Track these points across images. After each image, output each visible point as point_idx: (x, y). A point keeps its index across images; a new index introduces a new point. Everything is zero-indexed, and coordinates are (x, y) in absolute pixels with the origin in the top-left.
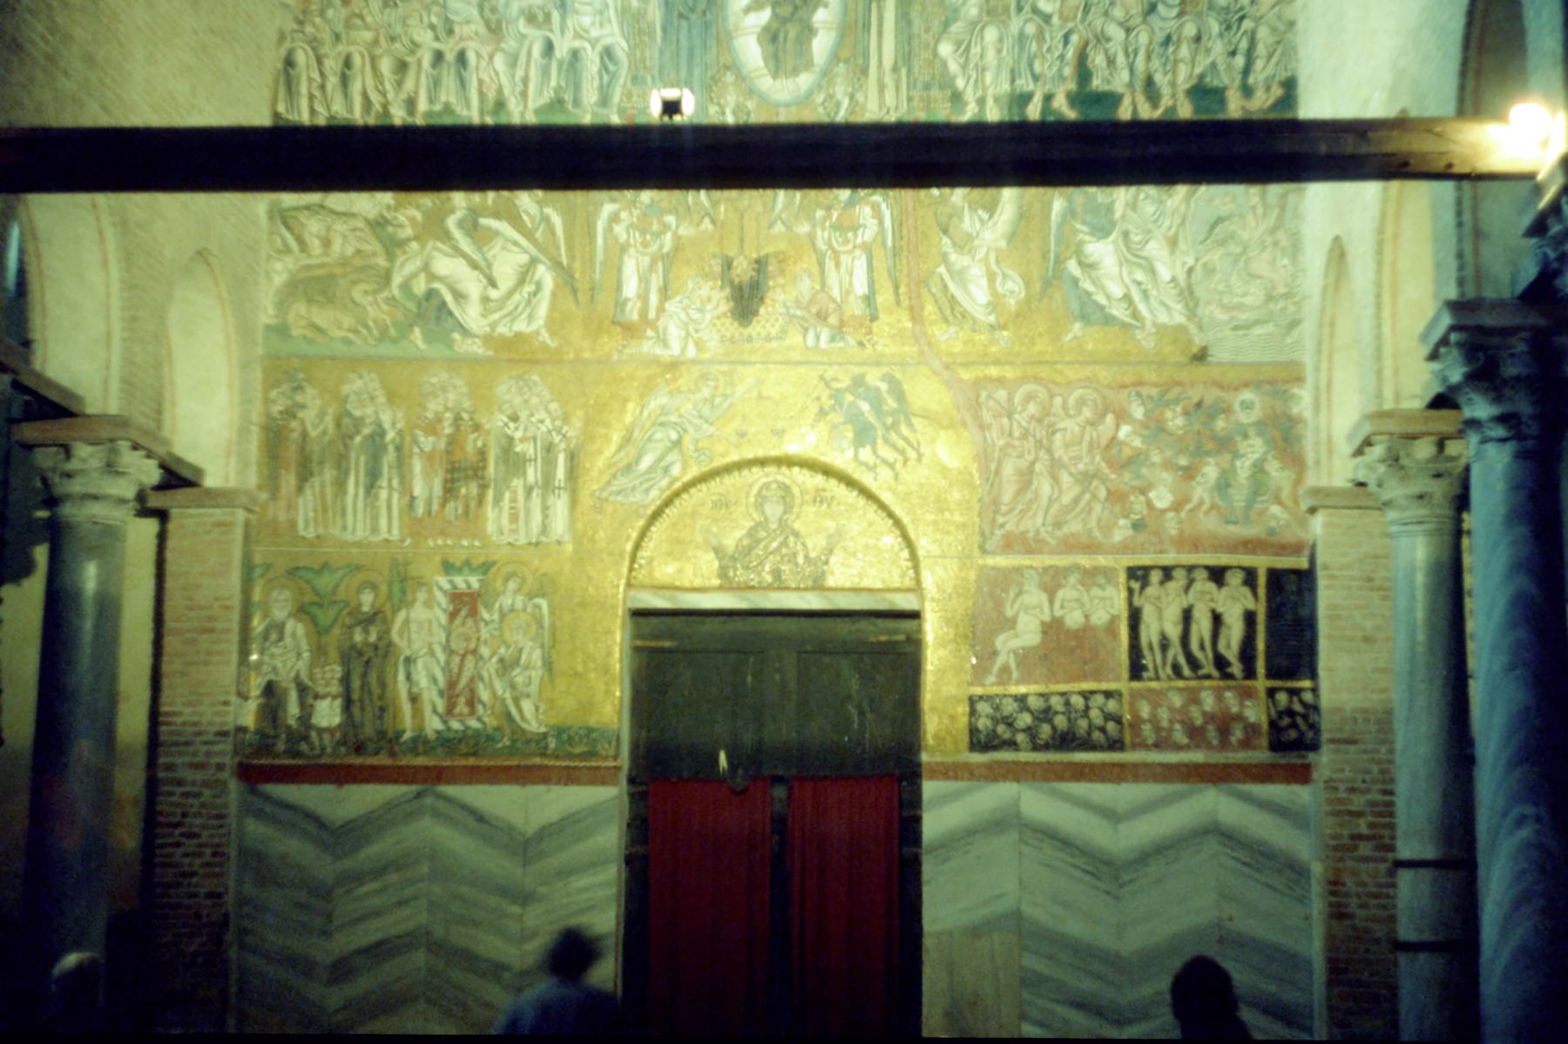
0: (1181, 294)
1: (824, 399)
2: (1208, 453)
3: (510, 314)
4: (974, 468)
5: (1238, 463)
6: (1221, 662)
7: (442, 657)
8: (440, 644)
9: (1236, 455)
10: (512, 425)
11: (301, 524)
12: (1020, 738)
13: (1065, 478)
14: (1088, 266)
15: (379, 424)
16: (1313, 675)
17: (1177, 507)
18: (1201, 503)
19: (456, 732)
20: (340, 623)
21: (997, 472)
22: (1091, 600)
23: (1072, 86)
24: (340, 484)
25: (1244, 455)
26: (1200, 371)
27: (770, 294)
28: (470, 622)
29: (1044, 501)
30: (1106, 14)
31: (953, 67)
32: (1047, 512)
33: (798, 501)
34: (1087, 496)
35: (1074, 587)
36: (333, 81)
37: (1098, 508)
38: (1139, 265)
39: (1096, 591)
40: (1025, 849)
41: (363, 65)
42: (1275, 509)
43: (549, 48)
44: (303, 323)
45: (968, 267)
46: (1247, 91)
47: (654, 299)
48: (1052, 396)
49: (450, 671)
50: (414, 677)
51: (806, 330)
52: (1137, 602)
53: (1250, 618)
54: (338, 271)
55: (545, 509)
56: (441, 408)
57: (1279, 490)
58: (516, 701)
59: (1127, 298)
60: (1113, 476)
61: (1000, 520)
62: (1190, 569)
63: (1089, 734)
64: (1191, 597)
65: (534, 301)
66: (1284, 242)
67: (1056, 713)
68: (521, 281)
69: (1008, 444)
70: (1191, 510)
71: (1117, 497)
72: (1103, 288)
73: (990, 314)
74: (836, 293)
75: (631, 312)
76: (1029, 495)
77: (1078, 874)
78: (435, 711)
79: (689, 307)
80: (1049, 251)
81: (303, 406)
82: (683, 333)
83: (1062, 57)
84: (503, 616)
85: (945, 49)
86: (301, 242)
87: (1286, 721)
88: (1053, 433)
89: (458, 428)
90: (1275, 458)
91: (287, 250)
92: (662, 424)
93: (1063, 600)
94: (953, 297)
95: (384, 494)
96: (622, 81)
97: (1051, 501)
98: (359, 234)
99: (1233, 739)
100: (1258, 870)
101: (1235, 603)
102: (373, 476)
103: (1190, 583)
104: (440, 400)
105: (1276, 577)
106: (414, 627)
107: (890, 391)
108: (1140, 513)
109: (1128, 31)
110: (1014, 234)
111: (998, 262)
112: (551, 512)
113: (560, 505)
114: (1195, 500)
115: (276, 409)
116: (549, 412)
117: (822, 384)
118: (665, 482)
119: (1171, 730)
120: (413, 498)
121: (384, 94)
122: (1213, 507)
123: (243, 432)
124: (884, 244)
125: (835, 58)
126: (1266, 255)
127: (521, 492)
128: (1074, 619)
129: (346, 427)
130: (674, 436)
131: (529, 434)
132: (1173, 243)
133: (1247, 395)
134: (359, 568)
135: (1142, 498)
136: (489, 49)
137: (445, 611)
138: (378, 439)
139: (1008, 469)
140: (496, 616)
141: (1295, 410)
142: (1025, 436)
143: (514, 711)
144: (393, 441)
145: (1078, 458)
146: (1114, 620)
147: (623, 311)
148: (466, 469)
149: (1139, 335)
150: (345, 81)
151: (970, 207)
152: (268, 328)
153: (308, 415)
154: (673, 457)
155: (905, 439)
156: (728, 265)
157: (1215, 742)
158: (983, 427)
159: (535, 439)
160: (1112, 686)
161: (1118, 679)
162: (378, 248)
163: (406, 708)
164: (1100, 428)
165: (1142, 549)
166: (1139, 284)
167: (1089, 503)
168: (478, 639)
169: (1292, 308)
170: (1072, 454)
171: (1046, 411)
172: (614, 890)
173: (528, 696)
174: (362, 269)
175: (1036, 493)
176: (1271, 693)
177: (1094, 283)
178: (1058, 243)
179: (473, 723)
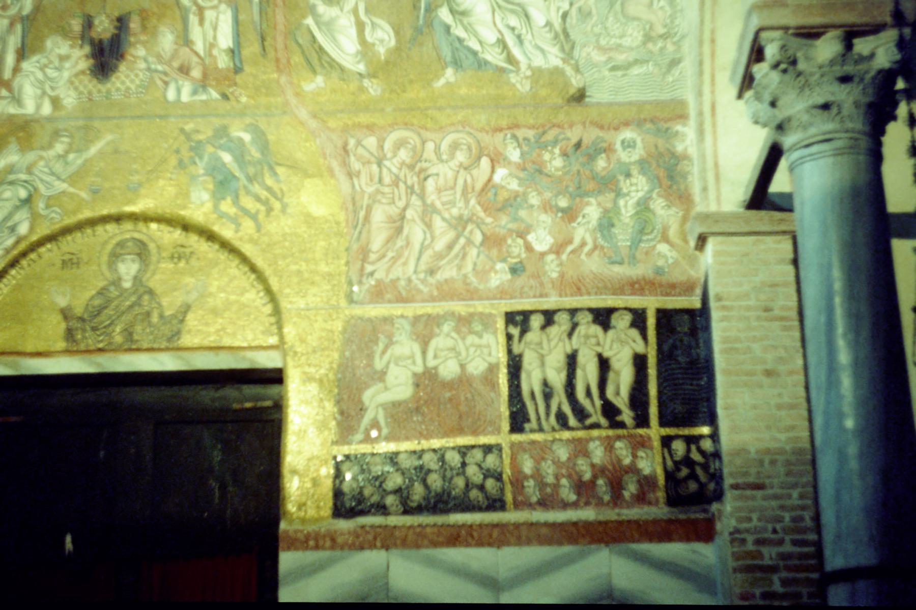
0: (556, 36)
2: (587, 194)
4: (342, 217)
5: (621, 202)
6: (610, 410)
9: (619, 194)
12: (390, 500)
13: (438, 224)
16: (712, 419)
17: (557, 249)
18: (583, 244)
21: (367, 219)
22: (467, 349)
25: (628, 194)
26: (577, 113)
27: (132, 51)
29: (417, 246)
32: (419, 259)
33: (154, 258)
35: (448, 335)
38: (513, 12)
39: (471, 339)
42: (663, 248)
45: (338, 17)
48: (424, 143)
51: (166, 83)
52: (516, 350)
53: (640, 362)
60: (489, 220)
61: (369, 268)
62: (573, 312)
64: (576, 342)
69: (378, 191)
70: (573, 252)
71: (492, 241)
72: (476, 35)
73: (359, 62)
74: (199, 47)
76: (400, 243)
79: (46, 66)
82: (39, 92)
87: (684, 472)
88: (425, 179)
90: (659, 195)
92: (12, 183)
93: (436, 350)
94: (321, 48)
97: (423, 249)
99: (626, 494)
103: (574, 326)
105: (664, 316)
107: (254, 141)
108: (519, 256)
111: (367, 11)
117: (182, 138)
118: (10, 242)
119: (556, 486)
122: (595, 247)
128: (449, 370)
130: (23, 194)
133: (628, 134)
135: (520, 241)
141: (679, 148)
142: (396, 183)
146: (492, 369)
149: (513, 78)
155: (269, 189)
156: (88, 24)
157: (607, 498)
158: (350, 175)
161: (498, 431)
164: (475, 172)
166: (513, 29)
167: (463, 248)
169: (670, 48)
170: (445, 199)
171: (418, 156)
175: (407, 237)
176: (666, 442)
177: (466, 30)
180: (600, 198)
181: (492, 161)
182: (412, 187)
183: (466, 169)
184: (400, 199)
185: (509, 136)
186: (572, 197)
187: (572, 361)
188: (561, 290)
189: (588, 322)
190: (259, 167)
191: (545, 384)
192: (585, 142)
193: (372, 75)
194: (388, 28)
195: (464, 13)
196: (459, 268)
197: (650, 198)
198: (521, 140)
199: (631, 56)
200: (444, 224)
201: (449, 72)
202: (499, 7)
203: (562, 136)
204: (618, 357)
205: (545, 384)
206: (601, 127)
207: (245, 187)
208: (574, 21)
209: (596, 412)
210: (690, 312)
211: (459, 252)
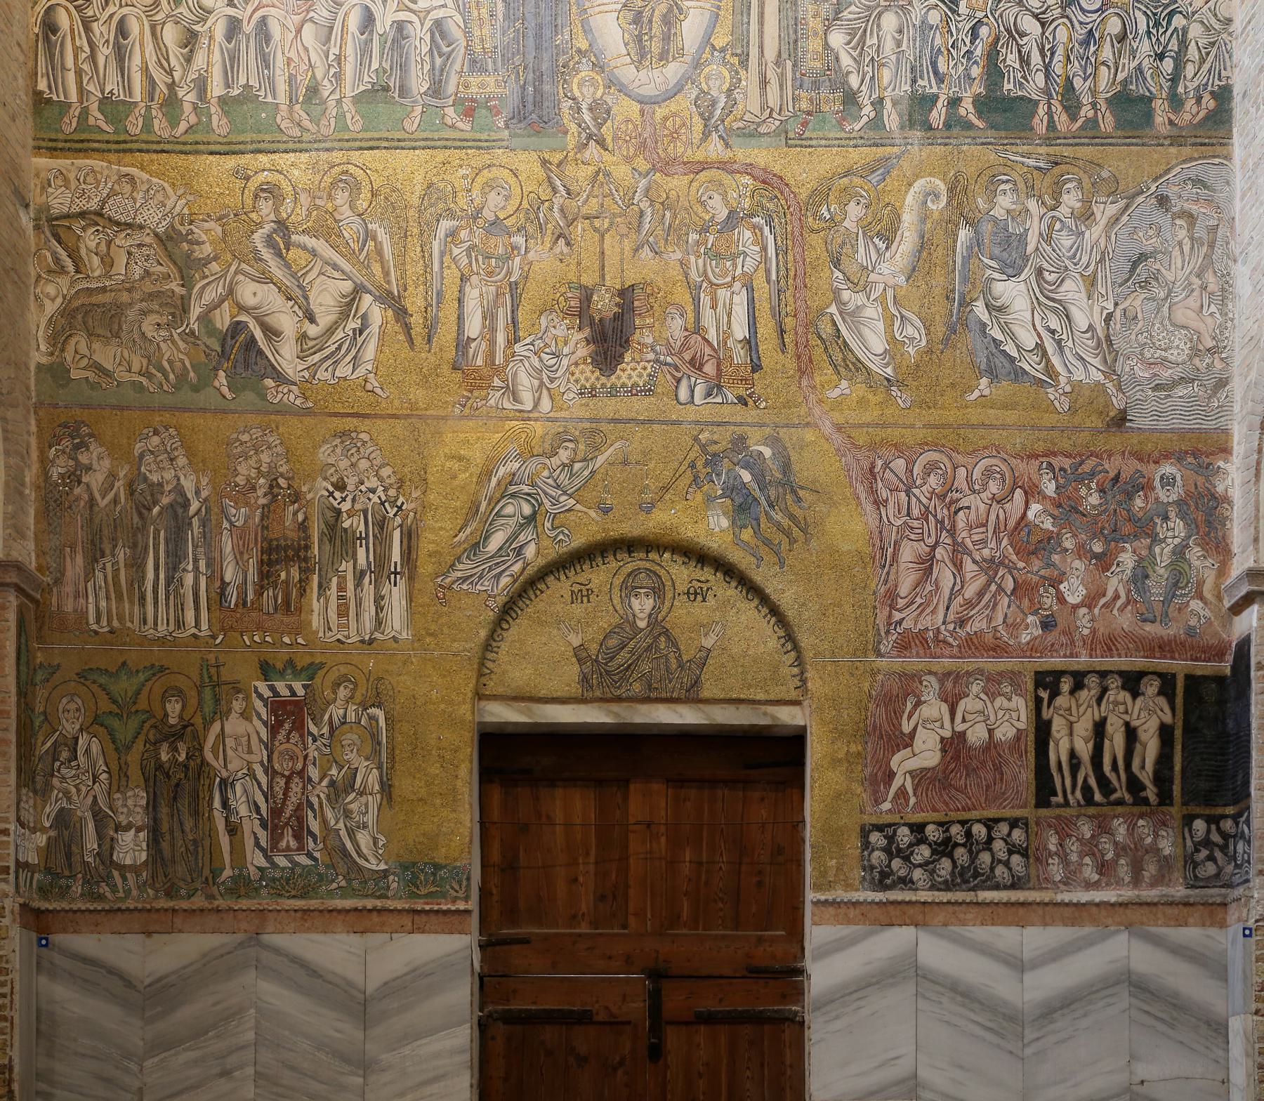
0: (1099, 345)
1: (699, 464)
3: (333, 353)
6: (1134, 785)
7: (263, 780)
8: (262, 763)
9: (1155, 539)
10: (337, 494)
11: (92, 619)
12: (917, 874)
13: (969, 566)
14: (996, 309)
15: (179, 490)
17: (1089, 602)
18: (1117, 597)
19: (283, 869)
20: (142, 737)
23: (977, 88)
24: (137, 565)
25: (1164, 541)
26: (1116, 441)
27: (636, 336)
28: (295, 736)
29: (947, 592)
31: (846, 61)
32: (948, 608)
34: (993, 587)
36: (104, 52)
37: (1006, 600)
38: (1054, 310)
40: (922, 1004)
41: (142, 33)
42: (1196, 605)
44: (85, 362)
46: (1176, 102)
47: (501, 339)
49: (273, 796)
50: (232, 803)
51: (679, 381)
52: (1046, 715)
53: (1165, 732)
54: (125, 297)
55: (379, 599)
56: (253, 473)
57: (1200, 584)
58: (351, 834)
59: (1040, 346)
60: (1021, 565)
61: (897, 616)
62: (1103, 674)
63: (992, 869)
65: (360, 340)
66: (1211, 287)
67: (956, 845)
68: (345, 315)
72: (1013, 337)
73: (887, 365)
74: (712, 335)
75: (475, 356)
76: (929, 588)
77: (979, 1031)
78: (257, 844)
80: (953, 291)
81: (89, 468)
82: (536, 383)
84: (332, 731)
85: (837, 39)
86: (74, 255)
88: (956, 513)
91: (62, 270)
92: (513, 496)
94: (844, 341)
95: (189, 579)
96: (457, 67)
98: (145, 251)
100: (1172, 1026)
103: (1104, 690)
104: (252, 462)
106: (230, 742)
110: (914, 269)
112: (385, 602)
113: (396, 595)
114: (1110, 594)
115: (55, 473)
116: (381, 479)
118: (517, 568)
120: (224, 585)
121: (170, 72)
122: (1128, 602)
124: (768, 272)
126: (1193, 302)
127: (350, 577)
130: (527, 510)
131: (357, 507)
132: (1091, 283)
133: (1168, 469)
134: (162, 669)
136: (297, 19)
137: (265, 723)
138: (180, 511)
139: (908, 553)
140: (325, 730)
141: (1220, 489)
142: (925, 516)
143: (349, 845)
144: (200, 510)
145: (984, 542)
146: (1020, 733)
147: (465, 354)
148: (286, 548)
151: (864, 234)
152: (40, 367)
153: (95, 480)
155: (792, 517)
156: (587, 296)
157: (1127, 879)
158: (878, 503)
159: (365, 512)
160: (1018, 813)
162: (174, 272)
163: (224, 840)
165: (1052, 649)
166: (1053, 332)
168: (306, 757)
169: (1218, 365)
170: (976, 538)
172: (467, 1057)
173: (365, 827)
174: (151, 296)
178: (965, 280)
179: (303, 860)
180: (1136, 543)
181: (1026, 493)
182: (942, 522)
183: (998, 502)
184: (929, 535)
185: (1045, 464)
186: (1107, 541)
187: (1099, 729)
188: (1092, 650)
189: (1117, 687)
190: (781, 490)
191: (1073, 754)
192: (1123, 475)
193: (901, 384)
194: (918, 323)
195: (1001, 309)
196: (990, 620)
197: (1187, 546)
198: (1057, 470)
200: (976, 568)
201: (984, 381)
202: (1039, 304)
203: (1101, 468)
204: (1145, 727)
205: (1073, 754)
206: (1141, 460)
207: (766, 513)
208: (1118, 326)
209: (1121, 787)
210: (1220, 680)
211: (990, 601)
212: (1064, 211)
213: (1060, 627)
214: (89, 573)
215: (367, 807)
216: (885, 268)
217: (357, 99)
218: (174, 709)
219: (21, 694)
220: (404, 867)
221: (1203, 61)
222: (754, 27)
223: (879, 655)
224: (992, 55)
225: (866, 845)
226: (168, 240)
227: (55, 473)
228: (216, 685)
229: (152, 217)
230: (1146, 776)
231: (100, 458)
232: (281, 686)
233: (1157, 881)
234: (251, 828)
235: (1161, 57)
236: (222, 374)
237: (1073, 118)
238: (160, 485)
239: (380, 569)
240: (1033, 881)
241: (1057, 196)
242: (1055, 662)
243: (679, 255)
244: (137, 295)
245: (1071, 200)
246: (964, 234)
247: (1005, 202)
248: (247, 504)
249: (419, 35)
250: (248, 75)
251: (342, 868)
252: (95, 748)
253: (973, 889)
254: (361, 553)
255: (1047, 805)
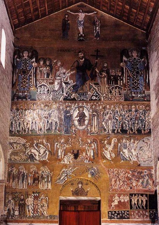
6: (143, 207)
9: (144, 178)
12: (115, 217)
14: (124, 153)
17: (136, 186)
18: (140, 185)
24: (18, 181)
28: (37, 200)
29: (118, 184)
30: (125, 119)
31: (104, 126)
42: (150, 186)
43: (48, 122)
46: (145, 131)
53: (146, 201)
54: (18, 151)
56: (33, 170)
57: (150, 184)
61: (112, 187)
62: (138, 194)
63: (125, 216)
68: (44, 153)
74: (89, 155)
81: (13, 170)
83: (119, 125)
84: (41, 200)
85: (103, 123)
89: (35, 173)
95: (24, 182)
101: (144, 199)
102: (23, 180)
103: (138, 196)
106: (29, 201)
109: (128, 122)
111: (111, 152)
113: (50, 184)
114: (139, 185)
115: (9, 170)
120: (29, 183)
121: (25, 127)
123: (5, 173)
124: (95, 149)
125: (88, 124)
126: (148, 152)
129: (19, 173)
130: (66, 175)
132: (135, 150)
133: (146, 171)
140: (41, 200)
141: (152, 173)
150: (19, 126)
153: (14, 171)
154: (66, 177)
155: (99, 176)
156: (73, 151)
169: (151, 159)
173: (45, 211)
178: (119, 149)
179: (38, 215)
186: (138, 179)
191: (135, 203)
199: (146, 160)
205: (135, 203)
212: (131, 142)
213: (133, 188)
214: (13, 182)
215: (45, 208)
216: (110, 148)
217: (46, 130)
218: (22, 197)
219: (5, 195)
220: (50, 216)
221: (147, 126)
222: (94, 122)
223: (110, 191)
224: (122, 125)
225: (108, 213)
226: (24, 145)
227: (9, 170)
228: (27, 194)
229: (22, 143)
230: (144, 206)
231: (15, 169)
232: (35, 195)
233: (146, 218)
234: (31, 211)
235: (142, 125)
236: (29, 160)
237: (132, 132)
238: (22, 172)
239: (48, 181)
240: (130, 218)
241: (130, 140)
242: (132, 193)
243: (84, 146)
244: (20, 151)
245: (132, 141)
246: (119, 144)
247: (124, 141)
248: (32, 174)
249: (54, 123)
250: (34, 127)
251: (42, 216)
252: (13, 201)
253: (123, 219)
254: (45, 179)
255: (132, 209)
